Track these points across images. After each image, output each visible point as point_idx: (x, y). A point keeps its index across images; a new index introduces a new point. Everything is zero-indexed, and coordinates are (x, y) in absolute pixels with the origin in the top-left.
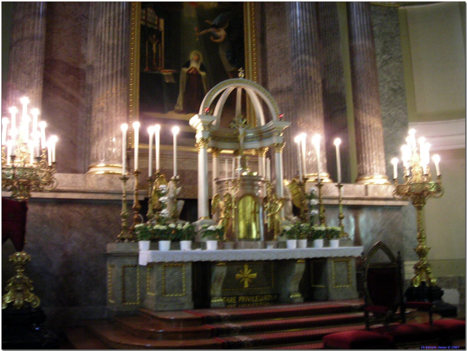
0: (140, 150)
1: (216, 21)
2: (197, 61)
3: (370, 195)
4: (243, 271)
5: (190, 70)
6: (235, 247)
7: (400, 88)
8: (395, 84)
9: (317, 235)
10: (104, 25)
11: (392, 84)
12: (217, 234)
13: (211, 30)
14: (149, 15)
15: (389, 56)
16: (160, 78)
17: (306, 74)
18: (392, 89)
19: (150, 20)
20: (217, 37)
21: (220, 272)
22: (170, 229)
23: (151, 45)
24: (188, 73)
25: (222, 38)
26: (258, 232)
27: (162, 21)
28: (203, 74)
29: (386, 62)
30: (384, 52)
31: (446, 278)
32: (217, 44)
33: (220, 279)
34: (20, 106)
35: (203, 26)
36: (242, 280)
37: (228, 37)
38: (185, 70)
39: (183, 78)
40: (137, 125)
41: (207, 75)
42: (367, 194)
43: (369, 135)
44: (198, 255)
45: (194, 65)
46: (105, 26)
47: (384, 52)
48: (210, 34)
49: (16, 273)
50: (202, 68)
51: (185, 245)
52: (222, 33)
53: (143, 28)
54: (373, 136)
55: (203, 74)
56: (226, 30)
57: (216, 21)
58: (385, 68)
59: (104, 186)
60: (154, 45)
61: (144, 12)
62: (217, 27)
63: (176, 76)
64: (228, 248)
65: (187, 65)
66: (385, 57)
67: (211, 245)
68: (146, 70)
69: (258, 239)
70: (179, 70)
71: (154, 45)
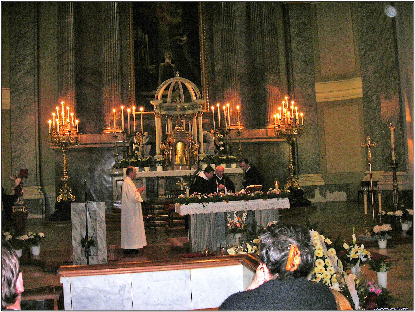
0: (136, 115)
2: (169, 58)
3: (269, 135)
4: (180, 181)
5: (165, 64)
6: (173, 169)
7: (309, 60)
8: (306, 58)
9: (223, 161)
10: (105, 51)
11: (303, 58)
12: (162, 163)
14: (139, 33)
15: (303, 39)
16: (147, 71)
17: (228, 64)
18: (304, 61)
19: (140, 36)
20: (181, 41)
22: (138, 161)
24: (164, 66)
25: (185, 41)
26: (186, 161)
27: (147, 36)
28: (173, 65)
29: (299, 43)
31: (339, 184)
32: (182, 46)
33: (162, 186)
34: (60, 106)
36: (179, 187)
38: (162, 64)
39: (161, 70)
40: (122, 108)
41: (176, 66)
42: (267, 135)
43: (271, 98)
44: (154, 174)
45: (167, 60)
46: (106, 52)
47: (298, 36)
48: (177, 40)
49: (64, 185)
50: (173, 62)
51: (147, 169)
52: (185, 38)
53: (135, 42)
54: (273, 99)
55: (173, 65)
56: (187, 36)
58: (298, 47)
59: (109, 139)
60: (143, 51)
61: (136, 31)
62: (181, 35)
63: (157, 68)
64: (169, 170)
66: (298, 39)
67: (160, 168)
69: (187, 165)
70: (159, 65)
71: (143, 51)
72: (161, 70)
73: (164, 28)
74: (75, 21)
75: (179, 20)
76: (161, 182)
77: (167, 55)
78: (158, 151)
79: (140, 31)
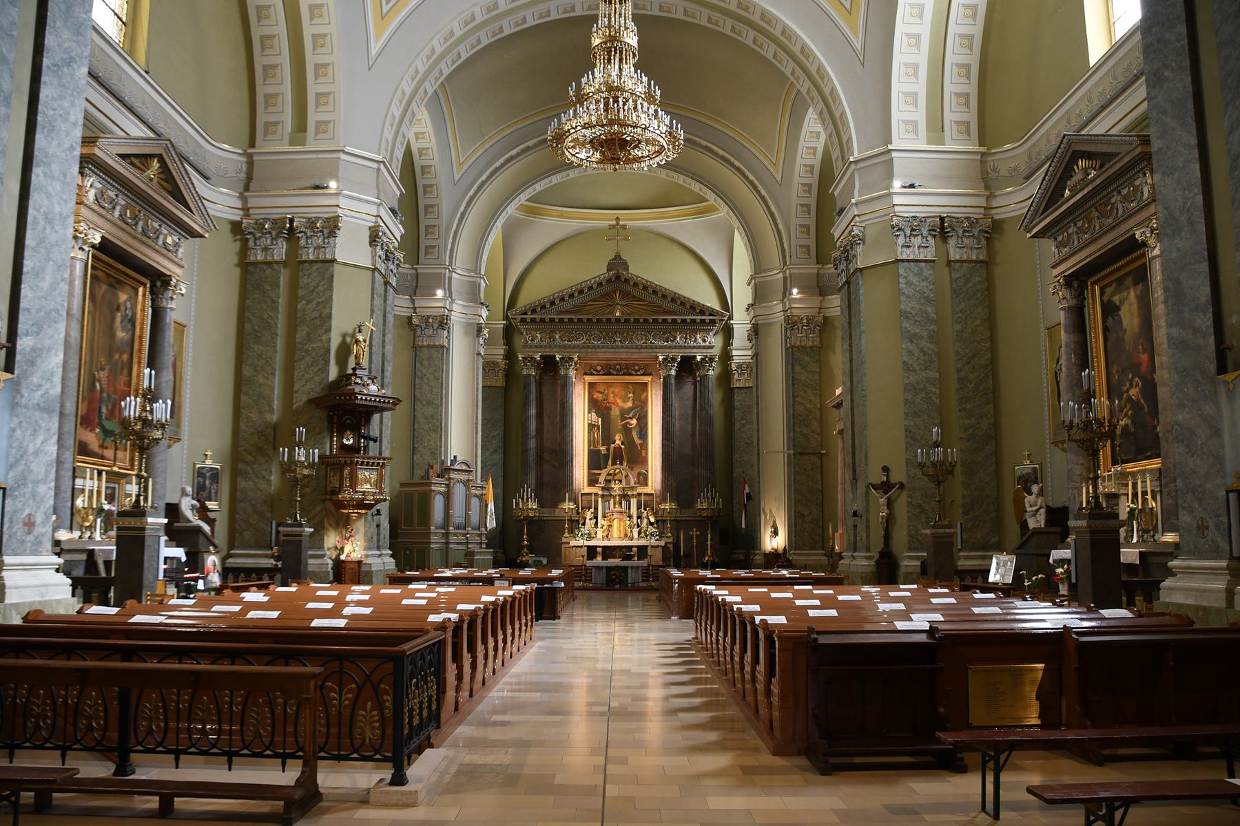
1: (631, 415)
13: (628, 420)
20: (631, 425)
21: (599, 550)
23: (594, 434)
27: (600, 419)
28: (623, 447)
30: (742, 418)
35: (623, 418)
37: (637, 424)
38: (613, 445)
39: (611, 450)
45: (618, 442)
47: (742, 418)
48: (628, 423)
52: (634, 422)
55: (623, 447)
57: (631, 415)
62: (631, 418)
63: (608, 450)
65: (614, 442)
68: (592, 447)
72: (611, 450)
73: (615, 412)
74: (537, 412)
75: (630, 404)
76: (599, 550)
77: (617, 437)
78: (599, 525)
79: (594, 414)
